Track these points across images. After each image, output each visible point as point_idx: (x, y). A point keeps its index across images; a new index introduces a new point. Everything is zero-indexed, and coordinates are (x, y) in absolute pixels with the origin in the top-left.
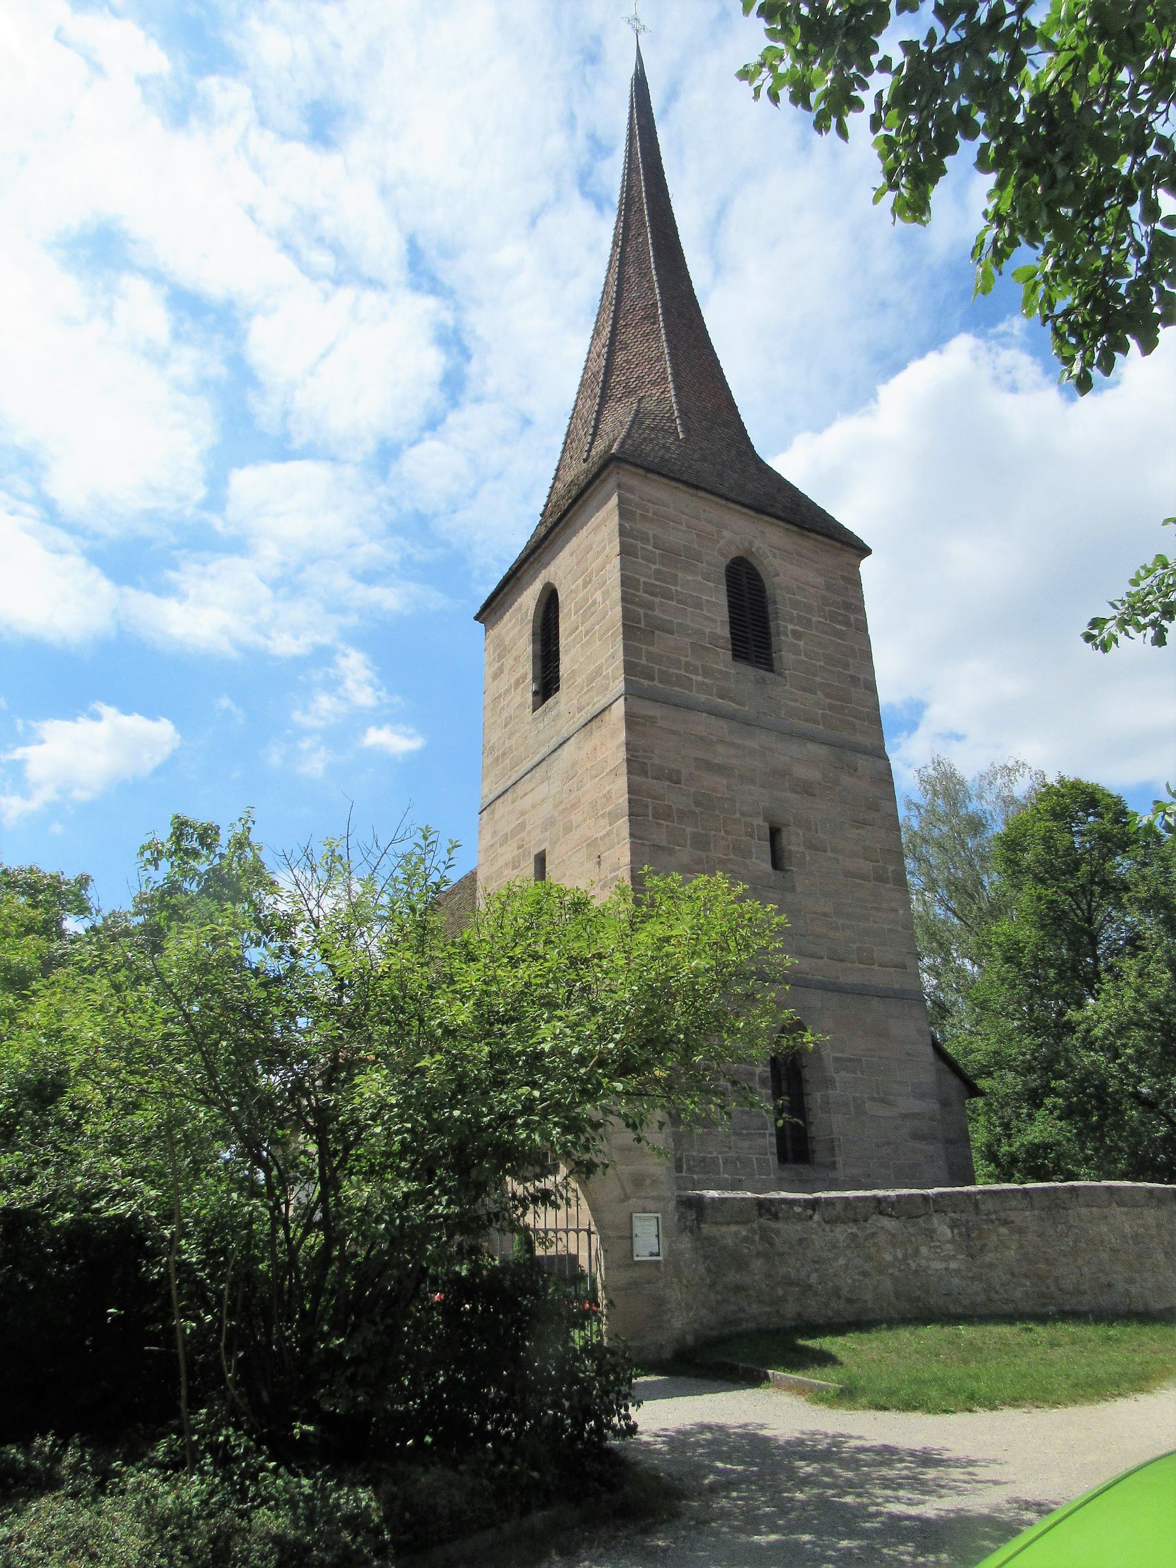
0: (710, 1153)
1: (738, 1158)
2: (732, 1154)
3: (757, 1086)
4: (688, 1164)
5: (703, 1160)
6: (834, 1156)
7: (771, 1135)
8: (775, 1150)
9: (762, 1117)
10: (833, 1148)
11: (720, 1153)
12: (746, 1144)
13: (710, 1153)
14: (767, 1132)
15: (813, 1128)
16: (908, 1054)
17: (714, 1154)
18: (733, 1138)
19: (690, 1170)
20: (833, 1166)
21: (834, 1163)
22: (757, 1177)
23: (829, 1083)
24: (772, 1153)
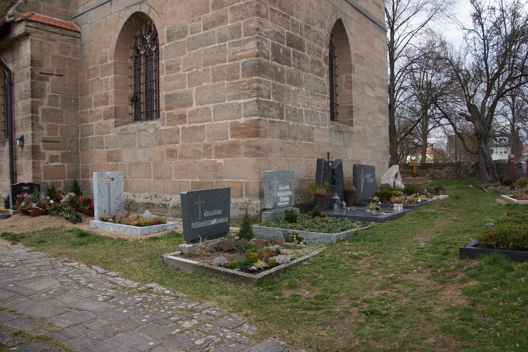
0: (299, 106)
1: (312, 112)
2: (310, 109)
3: (323, 62)
4: (287, 112)
5: (295, 111)
6: (352, 117)
7: (328, 97)
8: (329, 109)
9: (324, 84)
10: (352, 112)
11: (304, 107)
12: (316, 102)
13: (299, 106)
14: (327, 96)
15: (338, 98)
16: (380, 61)
17: (301, 108)
18: (310, 97)
19: (287, 117)
20: (351, 123)
21: (352, 121)
22: (321, 127)
23: (350, 69)
24: (328, 111)
